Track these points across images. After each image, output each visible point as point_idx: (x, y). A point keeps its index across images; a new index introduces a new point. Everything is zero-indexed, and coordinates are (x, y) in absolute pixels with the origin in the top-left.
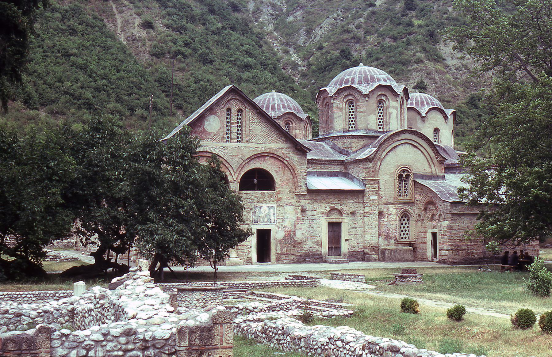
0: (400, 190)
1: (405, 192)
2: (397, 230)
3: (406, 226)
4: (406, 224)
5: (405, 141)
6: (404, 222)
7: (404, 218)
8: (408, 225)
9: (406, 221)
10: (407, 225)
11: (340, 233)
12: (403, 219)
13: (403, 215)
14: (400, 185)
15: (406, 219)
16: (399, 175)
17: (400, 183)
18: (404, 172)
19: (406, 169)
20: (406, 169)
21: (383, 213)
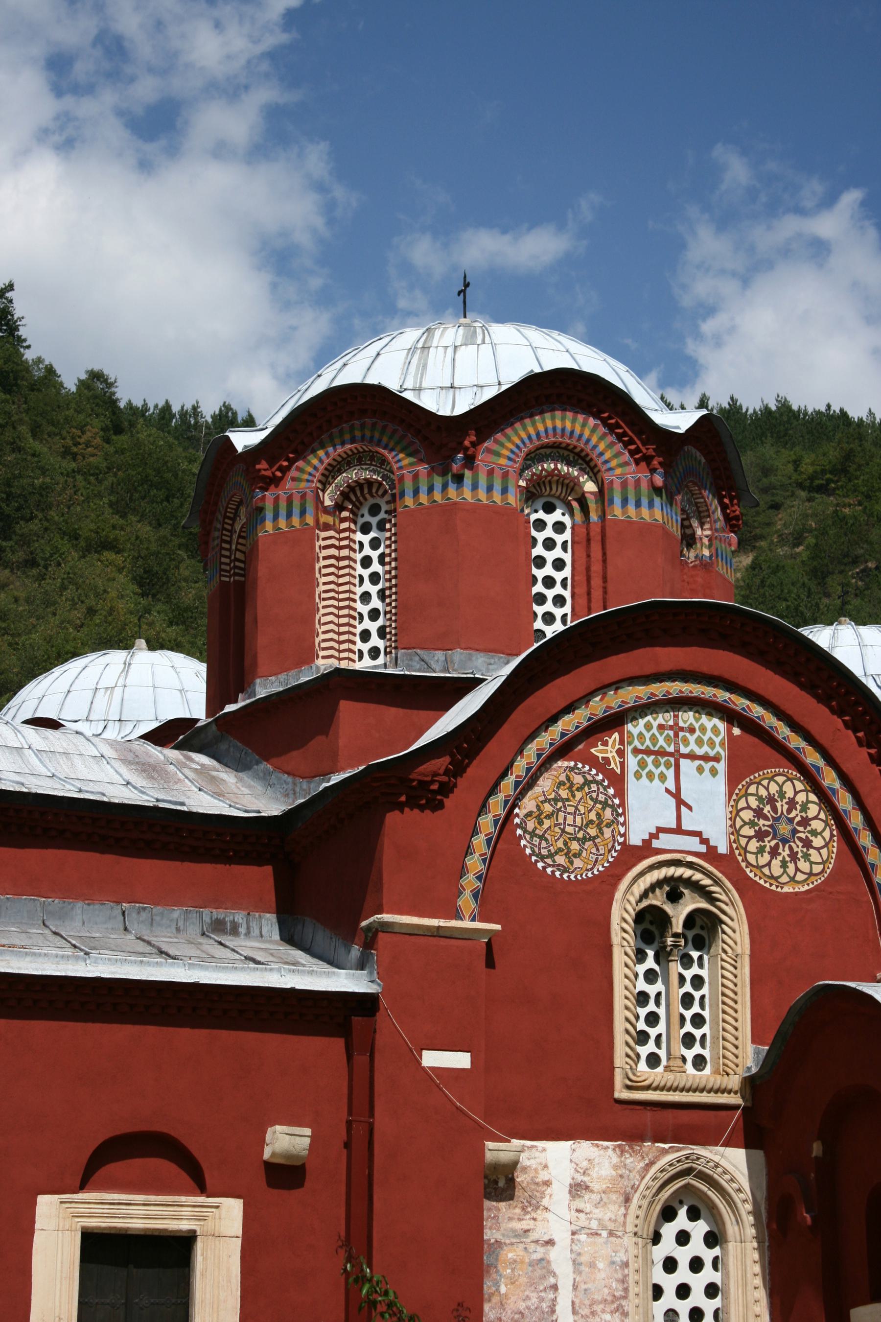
0: (652, 1019)
1: (689, 1040)
2: (629, 1305)
3: (698, 1282)
4: (696, 1265)
5: (676, 688)
6: (683, 1255)
7: (682, 1221)
8: (716, 1278)
9: (697, 1247)
10: (708, 1275)
11: (188, 1307)
12: (669, 1231)
13: (679, 1198)
14: (652, 990)
15: (699, 1229)
16: (640, 917)
17: (651, 977)
18: (674, 897)
19: (679, 871)
20: (687, 873)
21: (521, 1178)
